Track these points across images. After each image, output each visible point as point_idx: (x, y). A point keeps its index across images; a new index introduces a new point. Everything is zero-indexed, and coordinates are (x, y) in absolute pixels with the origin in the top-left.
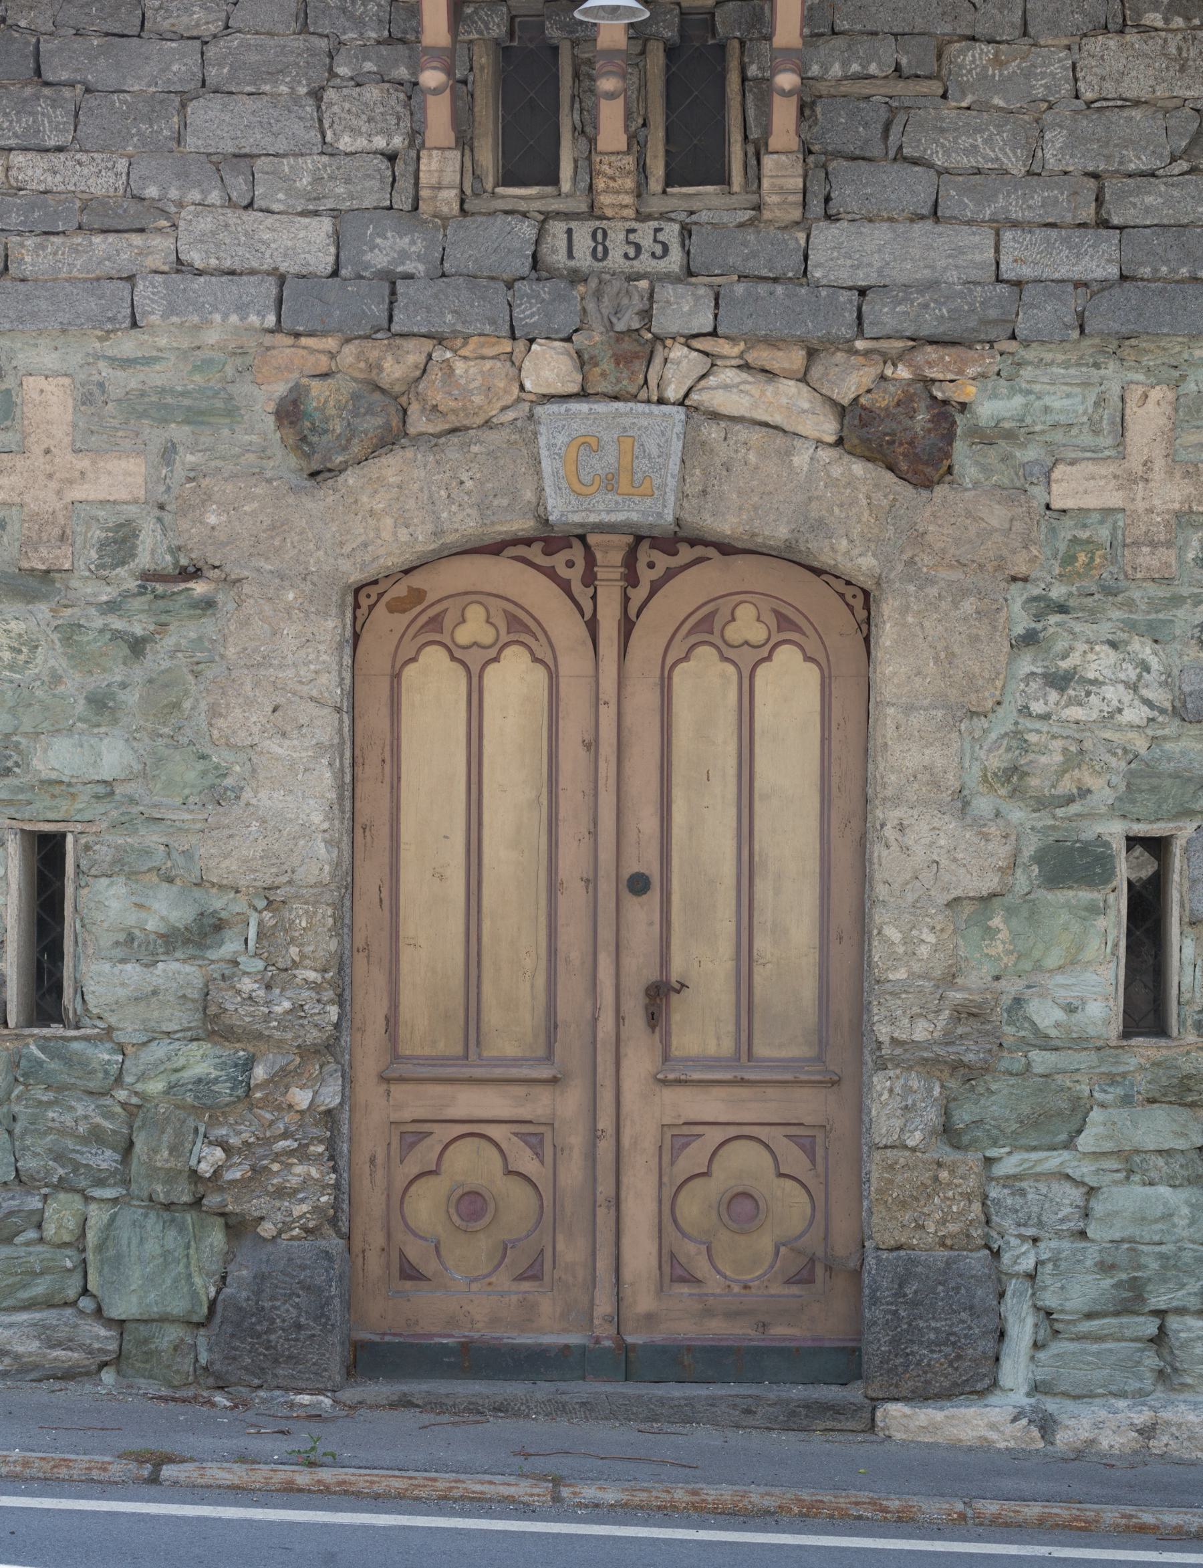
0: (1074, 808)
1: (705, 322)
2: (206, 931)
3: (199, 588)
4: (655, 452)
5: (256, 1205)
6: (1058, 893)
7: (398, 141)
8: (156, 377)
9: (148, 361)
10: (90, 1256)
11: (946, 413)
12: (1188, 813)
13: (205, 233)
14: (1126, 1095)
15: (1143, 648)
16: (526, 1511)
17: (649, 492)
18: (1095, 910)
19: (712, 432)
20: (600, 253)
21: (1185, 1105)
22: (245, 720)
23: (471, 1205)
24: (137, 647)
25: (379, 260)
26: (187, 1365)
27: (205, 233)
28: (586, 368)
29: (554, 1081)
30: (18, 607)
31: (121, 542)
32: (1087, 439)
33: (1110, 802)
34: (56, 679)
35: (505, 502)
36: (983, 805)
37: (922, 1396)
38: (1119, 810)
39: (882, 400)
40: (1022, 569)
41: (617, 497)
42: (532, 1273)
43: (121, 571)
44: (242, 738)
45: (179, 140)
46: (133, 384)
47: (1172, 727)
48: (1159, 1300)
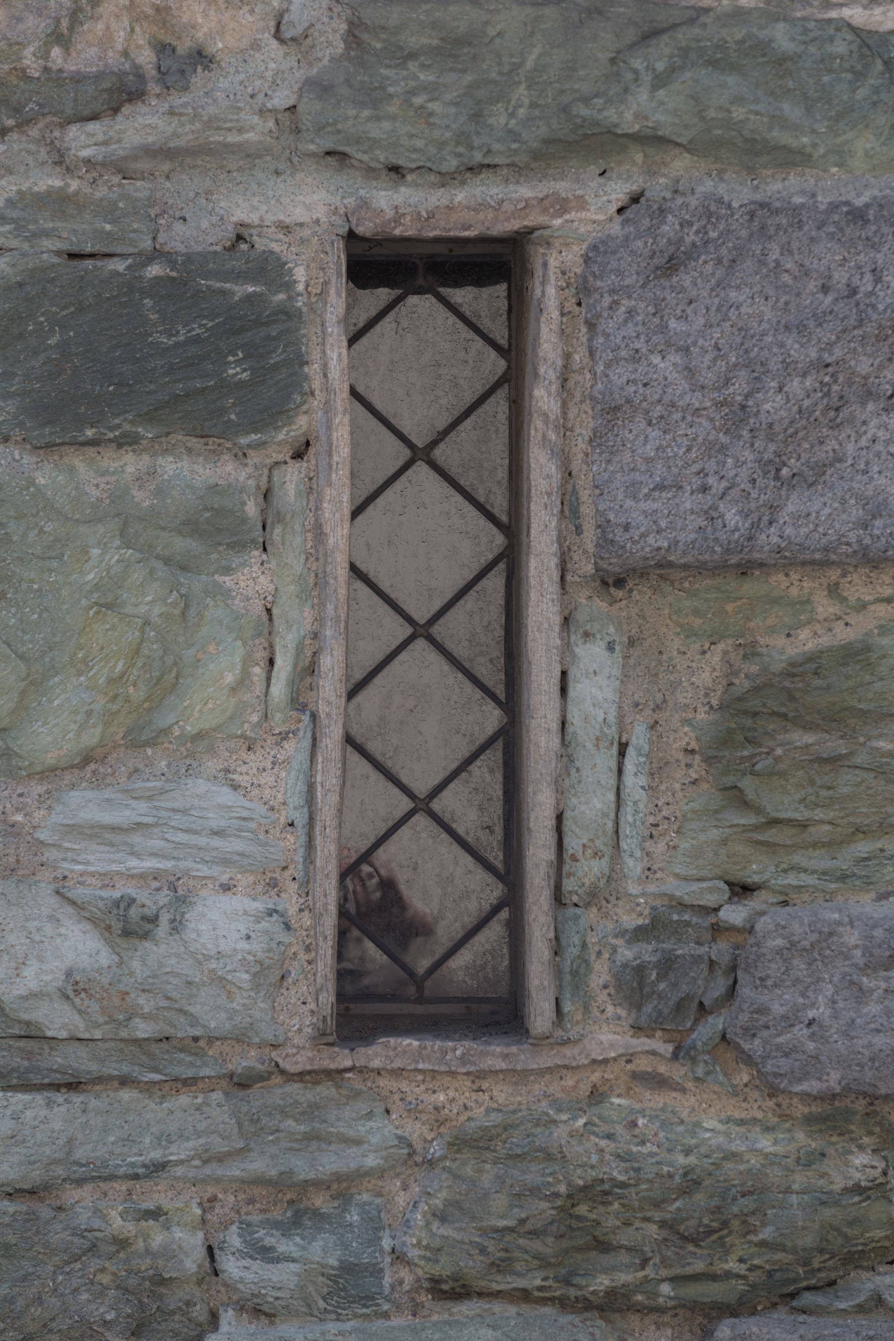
0: (141, 125)
6: (79, 462)
12: (590, 144)
14: (348, 1269)
18: (224, 531)
21: (586, 1305)
33: (282, 98)
38: (316, 137)
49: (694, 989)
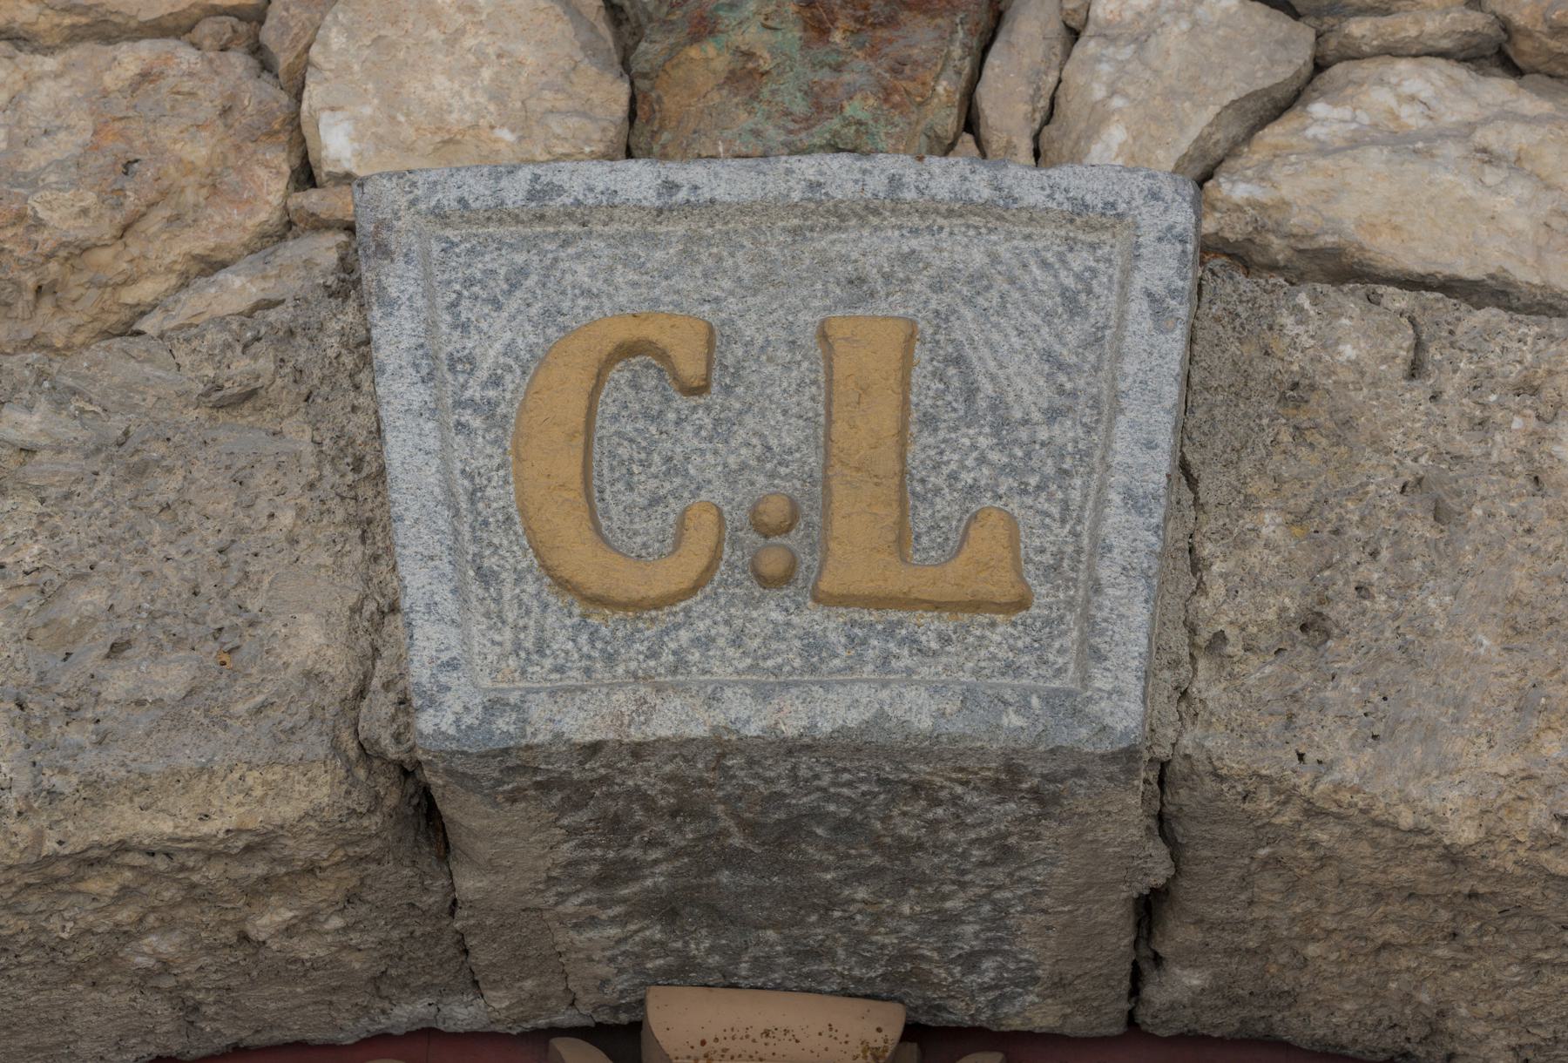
4: (1029, 391)
17: (1001, 586)
19: (1351, 341)
28: (650, 51)
35: (171, 677)
41: (813, 618)
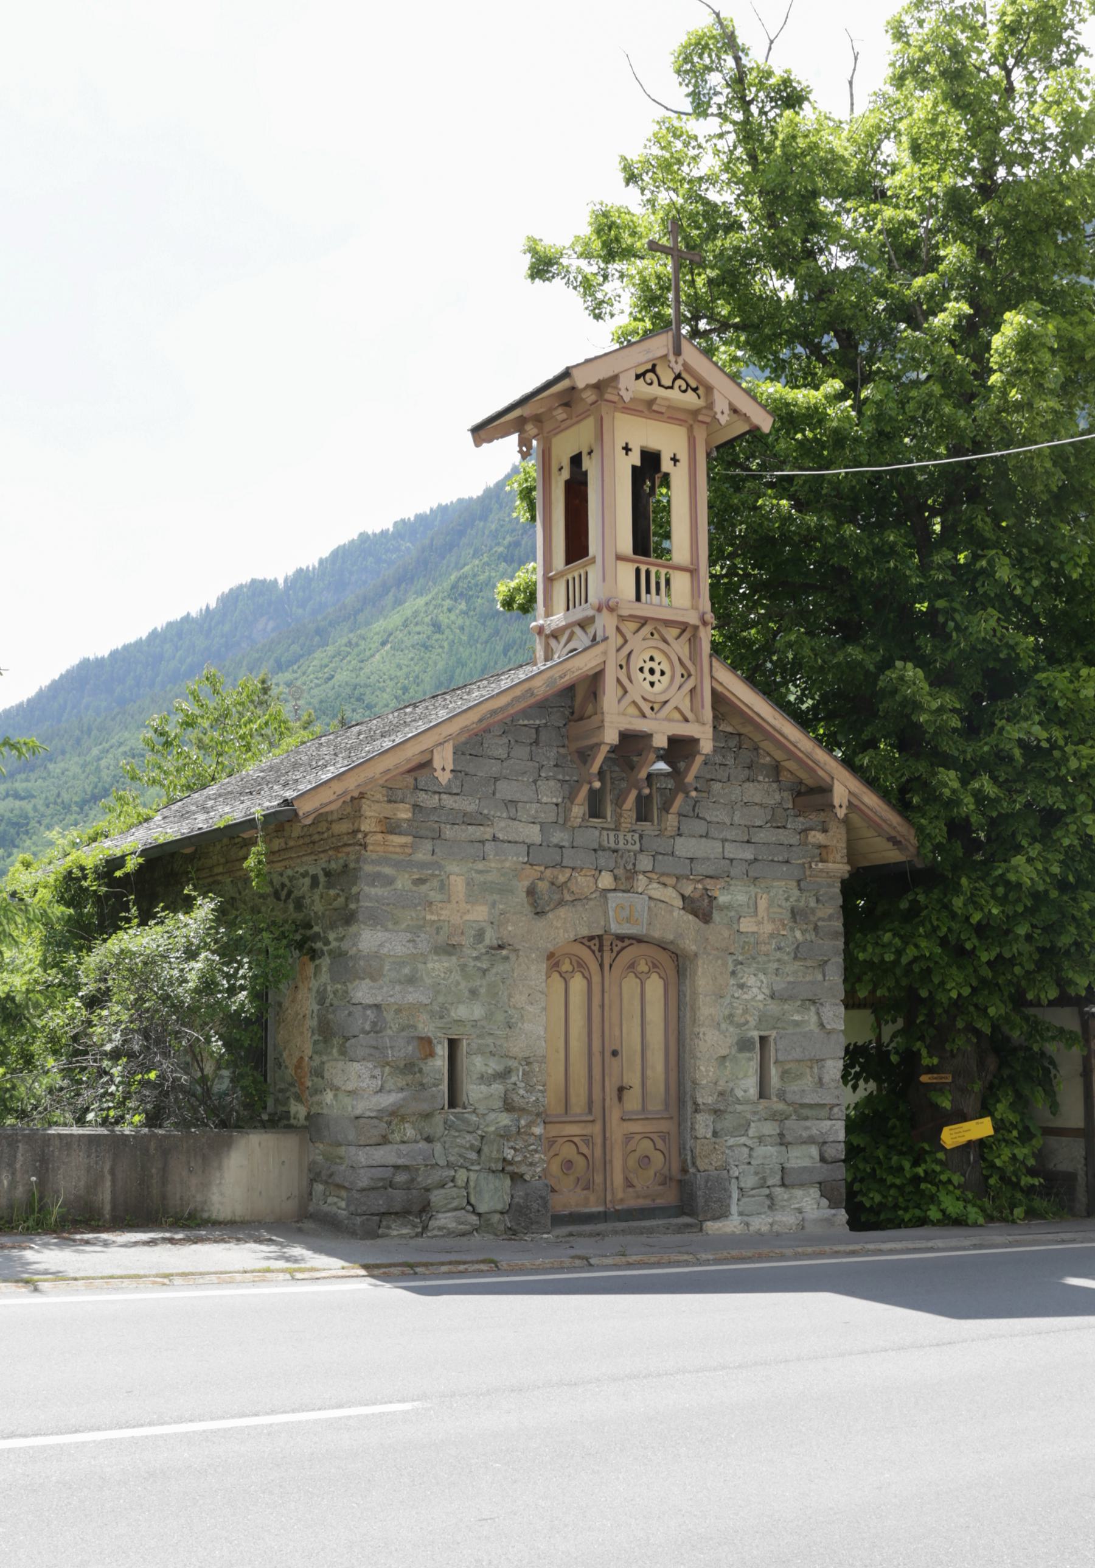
1: (650, 868)
2: (504, 1075)
3: (504, 952)
5: (523, 1169)
7: (560, 800)
8: (489, 877)
9: (488, 872)
10: (471, 1190)
11: (712, 899)
12: (774, 1028)
13: (502, 828)
15: (761, 976)
16: (687, 1264)
18: (750, 1059)
20: (617, 842)
22: (520, 999)
23: (568, 1164)
24: (484, 972)
25: (555, 840)
26: (502, 1227)
27: (502, 828)
29: (593, 1121)
30: (444, 958)
31: (480, 935)
32: (746, 910)
34: (458, 984)
36: (723, 1026)
37: (715, 1219)
39: (697, 895)
40: (732, 951)
42: (587, 1188)
43: (480, 946)
44: (519, 1005)
45: (494, 794)
46: (482, 879)
47: (769, 1001)
48: (769, 1183)
49: (782, 1096)
